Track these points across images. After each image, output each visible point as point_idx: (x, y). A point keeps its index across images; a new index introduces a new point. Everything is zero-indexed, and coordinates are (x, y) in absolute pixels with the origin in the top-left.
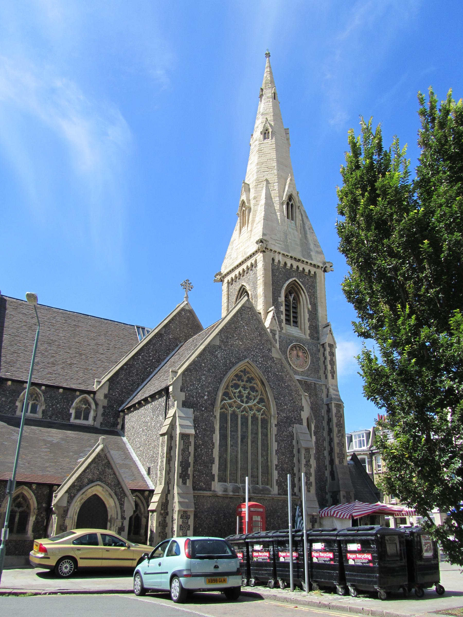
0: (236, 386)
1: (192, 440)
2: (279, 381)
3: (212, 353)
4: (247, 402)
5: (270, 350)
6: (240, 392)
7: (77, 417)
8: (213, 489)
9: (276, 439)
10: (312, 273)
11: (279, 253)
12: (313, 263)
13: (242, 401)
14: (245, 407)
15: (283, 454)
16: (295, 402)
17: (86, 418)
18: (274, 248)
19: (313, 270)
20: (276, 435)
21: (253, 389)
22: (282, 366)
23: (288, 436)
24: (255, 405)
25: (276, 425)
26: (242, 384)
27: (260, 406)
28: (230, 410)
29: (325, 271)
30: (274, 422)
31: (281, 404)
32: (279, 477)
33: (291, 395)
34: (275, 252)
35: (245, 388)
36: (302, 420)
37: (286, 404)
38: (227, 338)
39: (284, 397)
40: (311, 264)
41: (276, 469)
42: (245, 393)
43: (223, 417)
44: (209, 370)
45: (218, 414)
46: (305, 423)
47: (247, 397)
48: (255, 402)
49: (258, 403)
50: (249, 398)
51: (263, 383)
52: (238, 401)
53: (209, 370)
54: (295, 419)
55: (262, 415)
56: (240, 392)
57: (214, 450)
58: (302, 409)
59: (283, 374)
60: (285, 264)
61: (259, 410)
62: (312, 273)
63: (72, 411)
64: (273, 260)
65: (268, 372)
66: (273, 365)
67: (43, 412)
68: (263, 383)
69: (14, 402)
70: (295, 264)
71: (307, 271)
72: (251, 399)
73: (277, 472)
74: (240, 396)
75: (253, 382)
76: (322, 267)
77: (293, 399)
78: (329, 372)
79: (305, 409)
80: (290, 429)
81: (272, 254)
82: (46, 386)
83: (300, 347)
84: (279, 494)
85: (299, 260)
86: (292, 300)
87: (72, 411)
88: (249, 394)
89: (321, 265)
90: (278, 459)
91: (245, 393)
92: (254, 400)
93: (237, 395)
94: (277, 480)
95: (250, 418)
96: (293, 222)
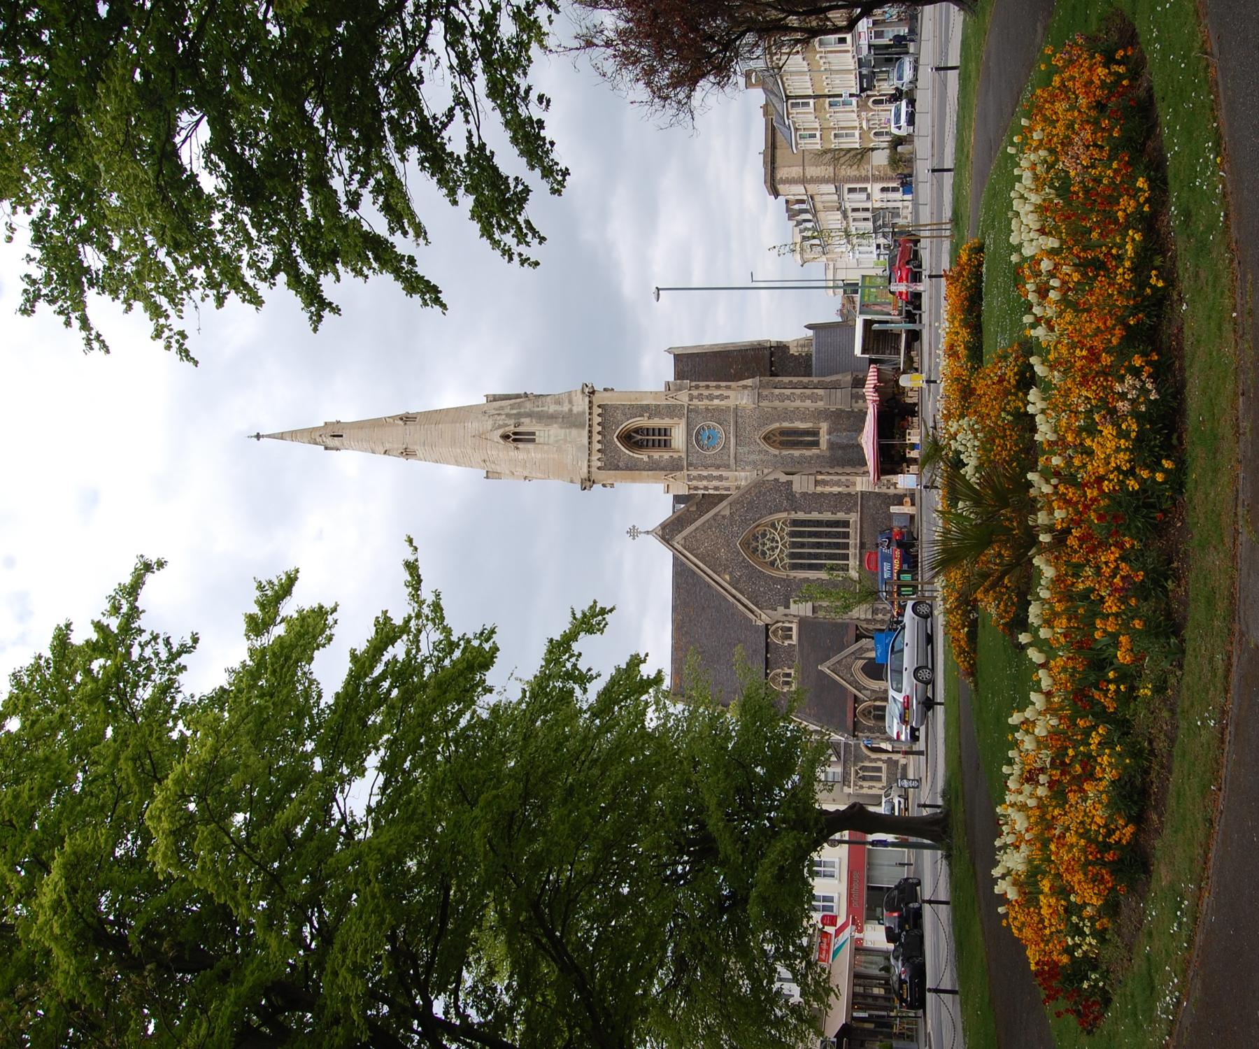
0: (764, 553)
1: (816, 604)
3: (738, 581)
4: (777, 542)
5: (724, 517)
6: (768, 549)
7: (790, 637)
10: (600, 411)
11: (589, 461)
12: (587, 408)
13: (777, 547)
17: (790, 629)
18: (585, 470)
19: (597, 411)
21: (764, 535)
26: (760, 547)
28: (787, 561)
29: (593, 392)
33: (765, 494)
34: (589, 466)
35: (764, 544)
37: (775, 499)
38: (720, 565)
40: (590, 414)
42: (769, 544)
43: (794, 567)
44: (753, 583)
45: (793, 574)
46: (790, 478)
49: (776, 530)
50: (773, 540)
51: (758, 526)
53: (753, 583)
56: (768, 549)
58: (776, 480)
60: (599, 451)
62: (600, 411)
63: (786, 643)
64: (599, 468)
67: (789, 668)
68: (758, 526)
69: (784, 694)
70: (597, 437)
71: (600, 419)
74: (773, 549)
78: (723, 403)
81: (594, 469)
82: (766, 669)
83: (698, 433)
85: (590, 432)
86: (640, 437)
87: (786, 643)
88: (768, 539)
89: (587, 399)
91: (769, 544)
96: (537, 433)
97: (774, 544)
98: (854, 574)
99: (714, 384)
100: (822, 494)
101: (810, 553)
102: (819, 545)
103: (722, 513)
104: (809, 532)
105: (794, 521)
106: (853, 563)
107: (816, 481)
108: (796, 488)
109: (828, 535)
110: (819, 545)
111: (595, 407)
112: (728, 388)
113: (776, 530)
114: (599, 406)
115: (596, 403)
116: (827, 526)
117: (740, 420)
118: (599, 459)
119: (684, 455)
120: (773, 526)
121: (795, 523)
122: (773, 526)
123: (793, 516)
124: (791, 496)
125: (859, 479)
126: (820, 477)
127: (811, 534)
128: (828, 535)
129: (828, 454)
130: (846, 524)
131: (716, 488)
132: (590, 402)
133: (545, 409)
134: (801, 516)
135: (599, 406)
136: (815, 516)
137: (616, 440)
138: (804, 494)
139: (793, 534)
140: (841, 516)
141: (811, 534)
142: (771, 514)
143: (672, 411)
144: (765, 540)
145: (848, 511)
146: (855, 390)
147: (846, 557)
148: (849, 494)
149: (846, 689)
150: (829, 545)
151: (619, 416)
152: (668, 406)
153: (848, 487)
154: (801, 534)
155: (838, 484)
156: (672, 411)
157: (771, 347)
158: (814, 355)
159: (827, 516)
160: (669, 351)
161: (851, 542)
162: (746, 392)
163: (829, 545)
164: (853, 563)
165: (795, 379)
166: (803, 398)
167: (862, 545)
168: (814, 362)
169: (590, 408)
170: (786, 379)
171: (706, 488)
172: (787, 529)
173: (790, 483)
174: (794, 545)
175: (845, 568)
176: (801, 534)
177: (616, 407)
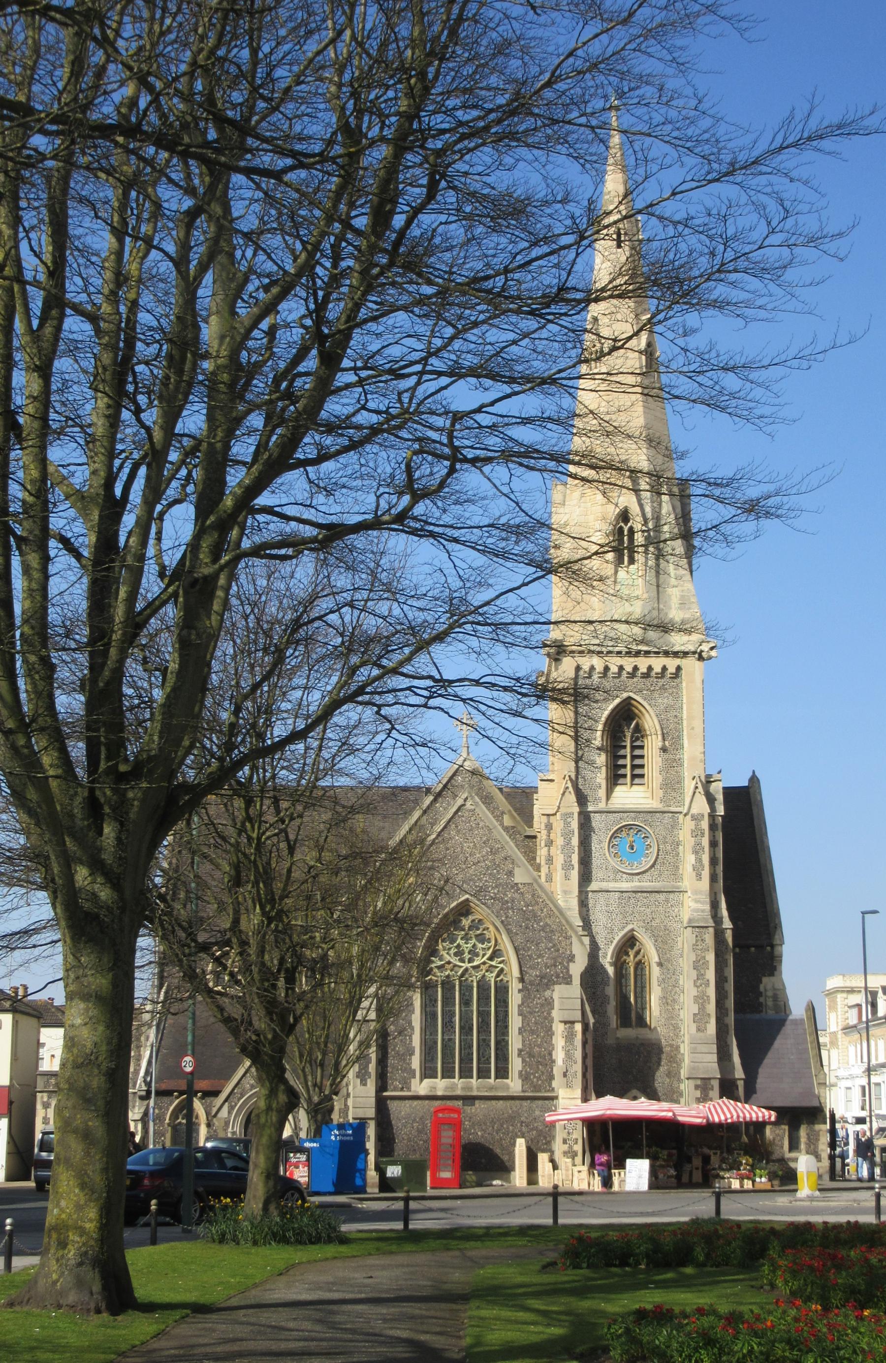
2: (528, 919)
4: (470, 961)
5: (510, 873)
8: (413, 1088)
9: (519, 1010)
10: (672, 669)
14: (466, 970)
15: (532, 1032)
16: (558, 950)
19: (672, 664)
20: (519, 1006)
21: (481, 938)
22: (533, 896)
23: (542, 1005)
24: (484, 963)
25: (520, 991)
27: (493, 963)
30: (515, 987)
31: (530, 956)
32: (524, 1067)
35: (466, 938)
36: (571, 977)
39: (537, 944)
41: (519, 1055)
42: (467, 947)
46: (577, 980)
47: (469, 953)
48: (485, 959)
49: (491, 958)
50: (474, 953)
52: (455, 961)
54: (558, 976)
55: (498, 976)
56: (459, 946)
57: (414, 1037)
58: (571, 958)
59: (536, 908)
61: (490, 969)
65: (508, 908)
66: (517, 896)
70: (628, 664)
72: (477, 955)
73: (520, 1059)
74: (459, 954)
75: (481, 927)
76: (694, 653)
77: (554, 946)
79: (577, 959)
80: (547, 993)
84: (523, 1091)
88: (474, 946)
89: (691, 648)
90: (523, 1041)
92: (484, 955)
93: (452, 952)
94: (520, 1072)
95: (475, 984)
96: (632, 567)
97: (467, 956)
98: (421, 1087)
99: (720, 855)
100: (550, 1033)
101: (453, 1014)
102: (466, 1029)
103: (517, 871)
104: (489, 1013)
105: (506, 989)
106: (440, 1085)
107: (573, 1023)
108: (558, 992)
109: (484, 1044)
110: (466, 1029)
111: (677, 662)
112: (713, 878)
113: (491, 958)
114: (679, 668)
115: (686, 663)
116: (497, 1043)
117: (662, 897)
118: (592, 668)
119: (602, 806)
120: (496, 954)
121: (502, 990)
122: (496, 954)
123: (515, 987)
124: (546, 982)
125: (578, 1093)
126: (578, 1027)
127: (484, 1016)
128: (484, 1044)
129: (610, 1041)
130: (502, 1072)
131: (550, 860)
132: (685, 654)
133: (673, 581)
134: (515, 999)
135: (679, 668)
136: (515, 1022)
137: (625, 695)
138: (549, 1003)
139: (483, 986)
140: (516, 1064)
141: (484, 1016)
142: (517, 950)
143: (672, 785)
144: (474, 941)
145: (525, 1077)
146: (716, 1084)
147: (448, 1073)
148: (551, 1077)
149: (228, 1078)
150: (466, 1046)
151: (664, 701)
152: (680, 781)
153: (565, 1075)
154: (484, 997)
155: (569, 1056)
156: (672, 785)
157: (772, 946)
158: (757, 1016)
159: (515, 1042)
160: (754, 779)
161: (474, 1081)
162: (707, 907)
163: (466, 1046)
164: (440, 1085)
165: (730, 987)
166: (700, 1000)
167: (469, 1100)
168: (748, 1016)
169: (676, 654)
170: (730, 972)
171: (550, 843)
172: (491, 977)
173: (567, 980)
174: (466, 989)
175: (428, 1072)
176: (484, 997)
177: (677, 697)
